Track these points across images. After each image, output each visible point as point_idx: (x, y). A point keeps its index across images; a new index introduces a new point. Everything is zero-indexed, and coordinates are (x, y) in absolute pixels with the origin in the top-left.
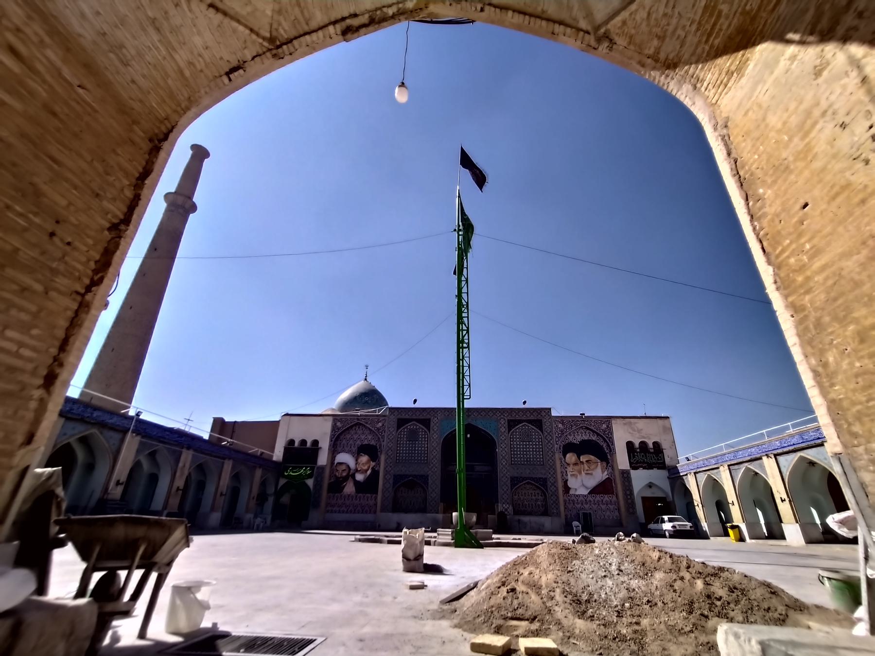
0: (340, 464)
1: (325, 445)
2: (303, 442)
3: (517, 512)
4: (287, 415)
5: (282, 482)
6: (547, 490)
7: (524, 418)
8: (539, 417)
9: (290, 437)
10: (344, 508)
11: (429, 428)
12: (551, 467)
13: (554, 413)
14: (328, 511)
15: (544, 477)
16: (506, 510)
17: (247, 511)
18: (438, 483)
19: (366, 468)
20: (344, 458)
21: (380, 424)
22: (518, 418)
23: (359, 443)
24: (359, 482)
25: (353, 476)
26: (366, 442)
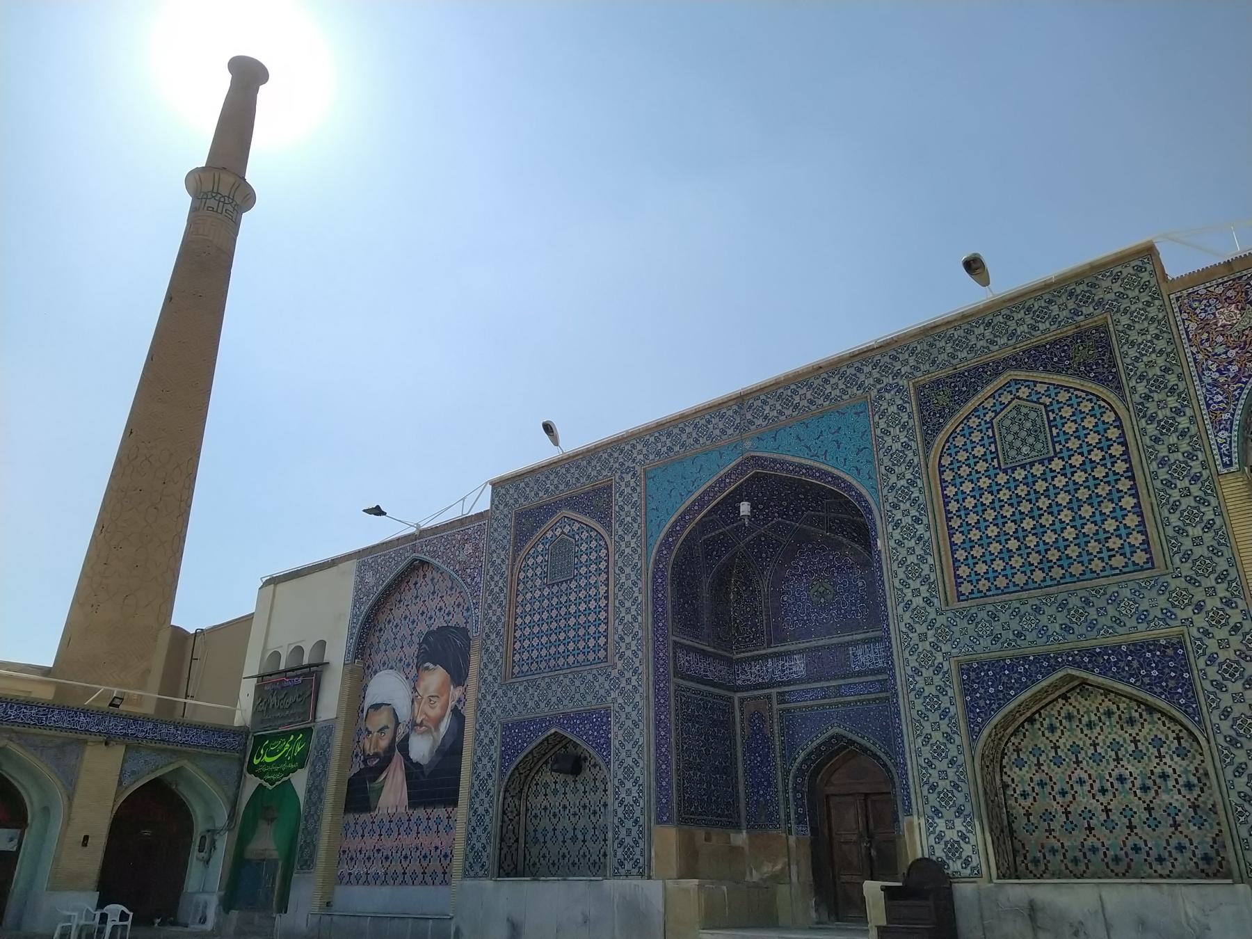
0: (377, 707)
1: (337, 655)
2: (299, 650)
3: (1016, 860)
4: (274, 581)
5: (251, 783)
6: (1195, 714)
7: (1003, 349)
8: (1091, 316)
9: (272, 647)
10: (377, 868)
11: (604, 517)
12: (1204, 566)
13: (1178, 263)
14: (340, 879)
15: (1161, 633)
16: (953, 849)
17: (64, 882)
18: (645, 735)
19: (434, 712)
20: (388, 687)
21: (469, 548)
22: (967, 360)
23: (422, 628)
24: (418, 765)
25: (404, 747)
26: (439, 623)
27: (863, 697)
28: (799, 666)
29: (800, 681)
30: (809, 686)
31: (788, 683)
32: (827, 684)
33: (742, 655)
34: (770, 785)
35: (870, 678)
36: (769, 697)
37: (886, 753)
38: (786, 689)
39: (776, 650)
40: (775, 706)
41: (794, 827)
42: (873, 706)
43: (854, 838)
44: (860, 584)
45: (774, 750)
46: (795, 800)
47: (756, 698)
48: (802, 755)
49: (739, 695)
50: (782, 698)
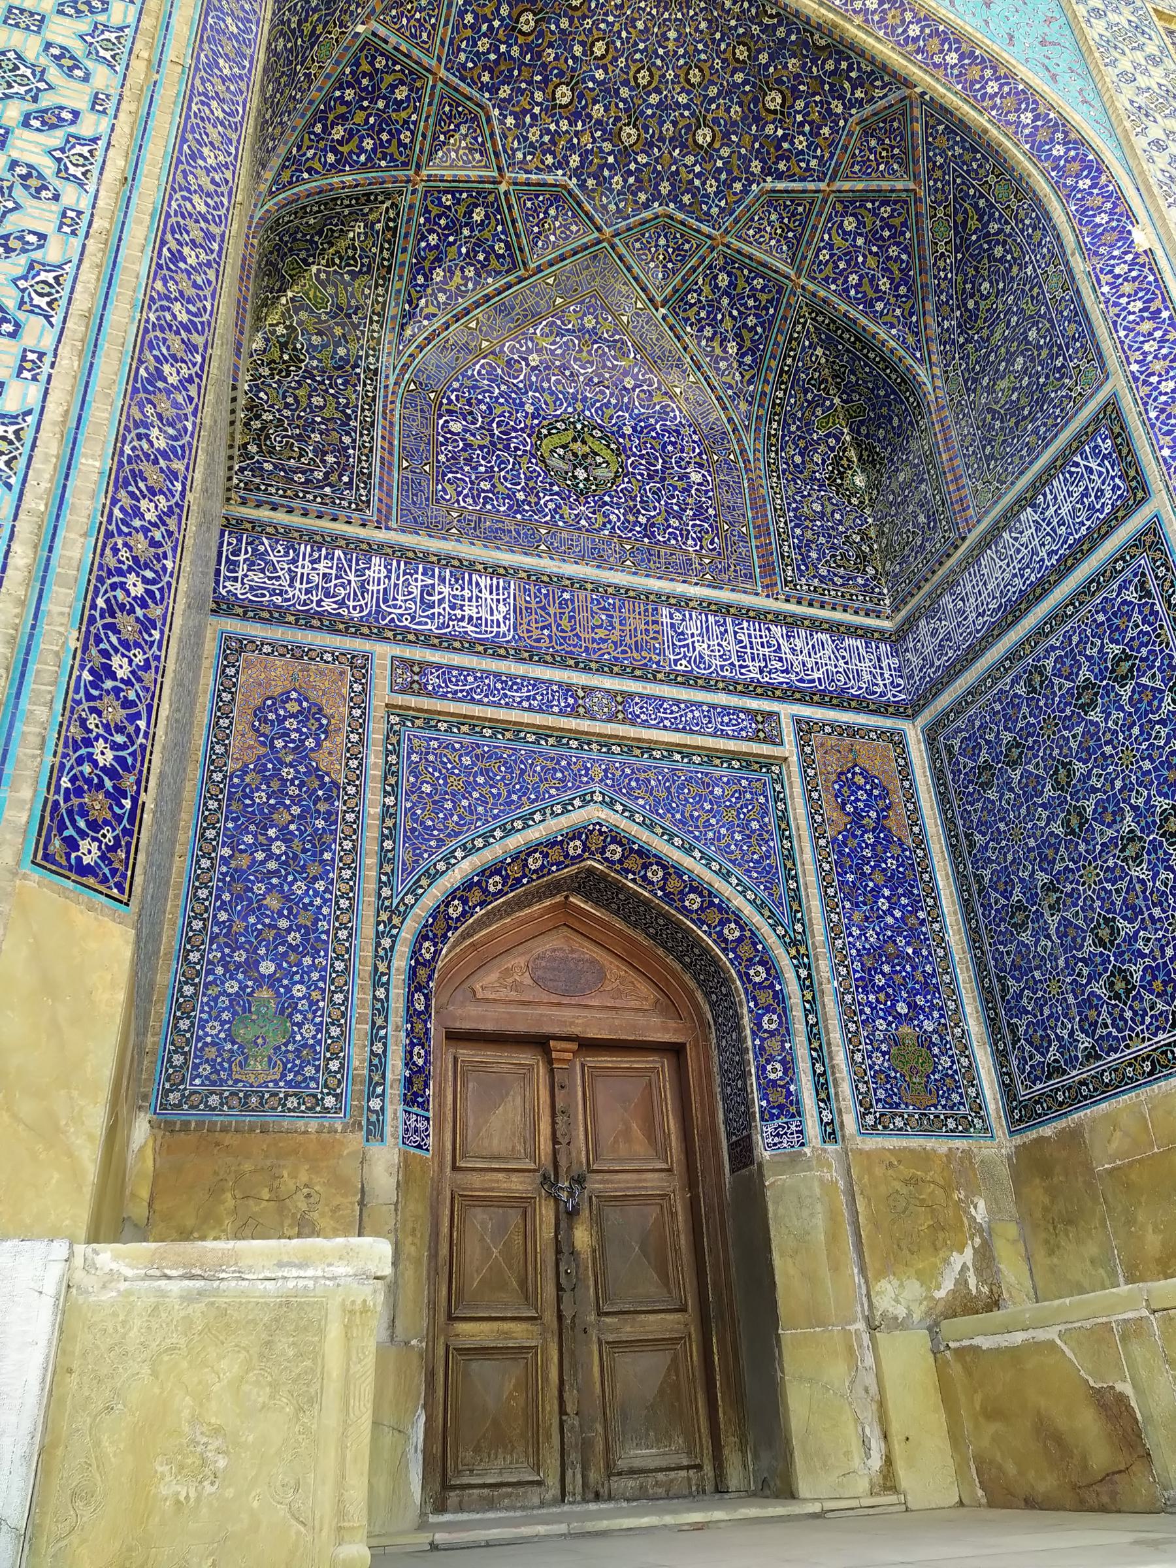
27: (699, 741)
28: (490, 608)
29: (492, 648)
30: (519, 669)
31: (445, 643)
32: (580, 679)
33: (264, 514)
34: (312, 943)
35: (722, 699)
36: (360, 665)
37: (760, 907)
38: (436, 657)
39: (408, 540)
40: (381, 693)
41: (394, 1111)
42: (721, 771)
43: (518, 1185)
44: (696, 477)
45: (356, 829)
46: (412, 1014)
47: (297, 652)
48: (465, 868)
49: (233, 625)
50: (412, 677)
